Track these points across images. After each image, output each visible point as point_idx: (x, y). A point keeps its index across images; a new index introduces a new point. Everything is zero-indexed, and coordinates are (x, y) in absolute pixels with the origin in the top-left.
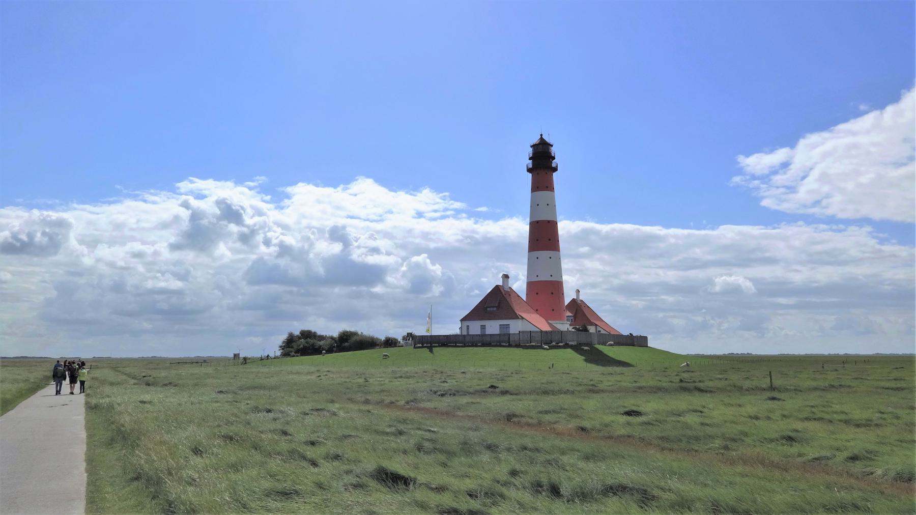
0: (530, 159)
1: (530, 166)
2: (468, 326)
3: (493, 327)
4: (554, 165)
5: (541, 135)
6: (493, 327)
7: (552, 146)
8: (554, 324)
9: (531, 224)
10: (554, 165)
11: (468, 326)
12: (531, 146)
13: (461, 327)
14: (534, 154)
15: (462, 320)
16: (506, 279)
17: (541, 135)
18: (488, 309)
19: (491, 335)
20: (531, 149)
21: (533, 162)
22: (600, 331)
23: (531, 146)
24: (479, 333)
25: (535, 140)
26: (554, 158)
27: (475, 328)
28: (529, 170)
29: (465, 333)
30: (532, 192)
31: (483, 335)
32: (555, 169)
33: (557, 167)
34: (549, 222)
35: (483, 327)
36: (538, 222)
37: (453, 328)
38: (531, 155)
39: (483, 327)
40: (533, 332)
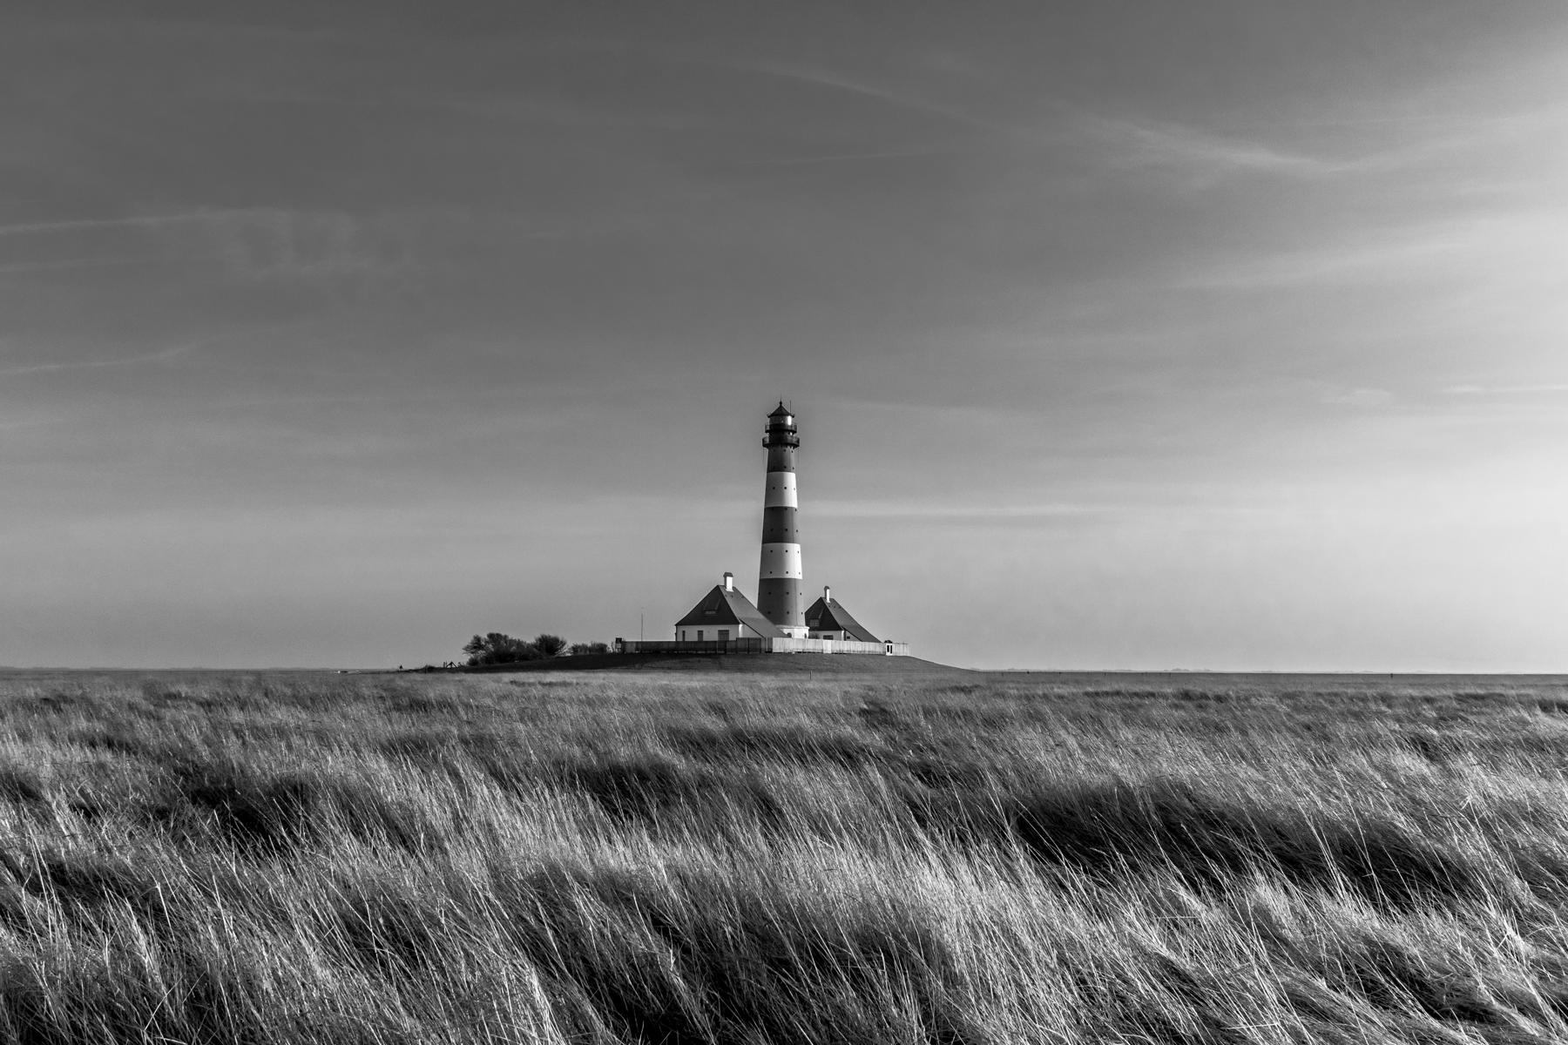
0: (767, 432)
1: (767, 441)
2: (684, 632)
3: (711, 633)
4: (794, 440)
5: (781, 403)
6: (711, 633)
11: (684, 632)
15: (676, 625)
17: (781, 403)
18: (707, 613)
19: (706, 642)
21: (771, 434)
24: (695, 638)
27: (692, 634)
28: (764, 445)
29: (680, 639)
31: (700, 641)
32: (796, 446)
33: (798, 441)
34: (786, 508)
35: (700, 633)
36: (773, 508)
37: (669, 635)
38: (768, 428)
39: (700, 633)
40: (752, 639)
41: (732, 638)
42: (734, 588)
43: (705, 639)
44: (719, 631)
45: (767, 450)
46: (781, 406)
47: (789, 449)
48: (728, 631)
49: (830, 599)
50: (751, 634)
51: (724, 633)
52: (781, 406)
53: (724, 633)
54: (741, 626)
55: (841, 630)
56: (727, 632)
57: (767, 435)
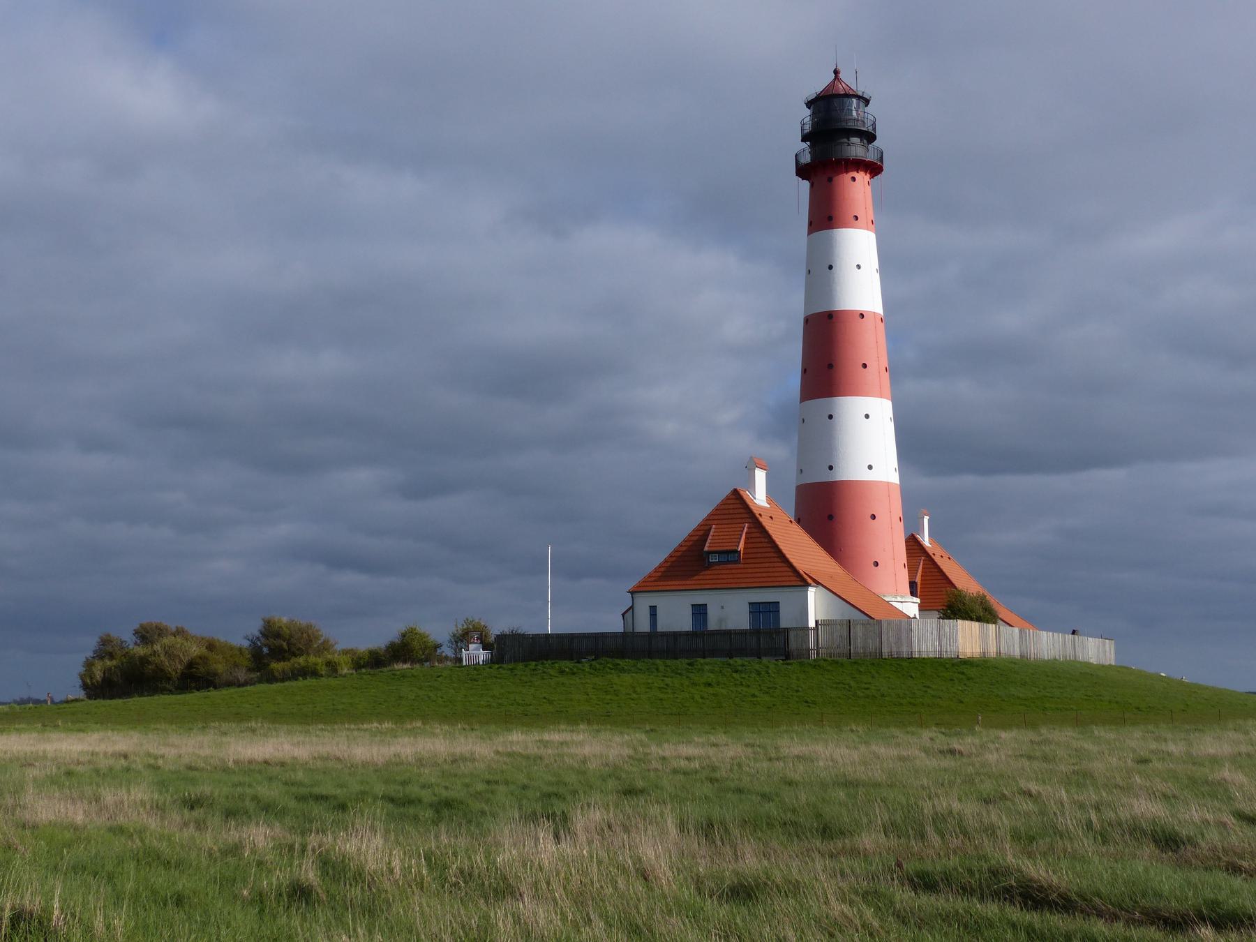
0: (804, 140)
2: (653, 609)
4: (871, 157)
5: (836, 72)
7: (867, 102)
8: (894, 604)
9: (807, 321)
11: (653, 609)
12: (809, 104)
13: (632, 607)
14: (814, 125)
15: (632, 593)
17: (836, 72)
20: (808, 112)
23: (809, 104)
25: (818, 84)
29: (643, 625)
30: (810, 232)
33: (881, 159)
35: (700, 612)
38: (808, 129)
39: (700, 612)
43: (712, 625)
47: (862, 177)
48: (779, 602)
50: (836, 612)
51: (765, 612)
53: (765, 612)
54: (812, 592)
56: (773, 608)
57: (806, 145)
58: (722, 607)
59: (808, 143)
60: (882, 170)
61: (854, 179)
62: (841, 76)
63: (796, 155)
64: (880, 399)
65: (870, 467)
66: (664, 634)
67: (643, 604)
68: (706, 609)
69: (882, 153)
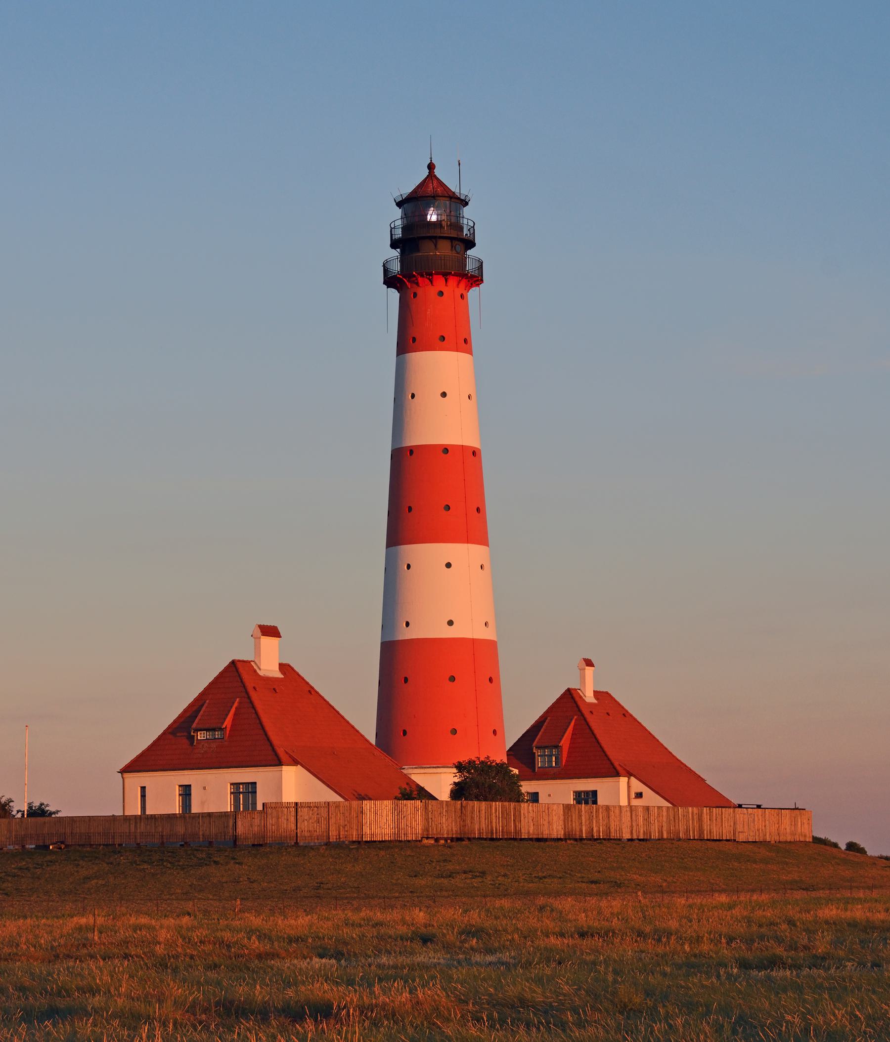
0: (394, 245)
1: (396, 267)
2: (143, 789)
5: (431, 167)
7: (466, 204)
10: (470, 266)
11: (143, 789)
14: (404, 229)
15: (123, 771)
16: (266, 641)
17: (431, 167)
20: (398, 212)
21: (402, 254)
22: (639, 795)
23: (399, 204)
24: (176, 808)
26: (470, 244)
28: (390, 281)
30: (397, 355)
32: (476, 280)
35: (186, 791)
36: (411, 450)
38: (398, 233)
39: (186, 791)
40: (309, 806)
41: (261, 799)
42: (284, 667)
44: (236, 785)
45: (394, 295)
46: (431, 176)
49: (597, 694)
52: (431, 176)
55: (617, 774)
57: (396, 253)
58: (205, 788)
59: (398, 250)
60: (482, 281)
61: (441, 293)
62: (437, 172)
63: (384, 266)
64: (465, 545)
65: (450, 623)
66: (153, 817)
67: (136, 780)
68: (190, 790)
69: (482, 263)
